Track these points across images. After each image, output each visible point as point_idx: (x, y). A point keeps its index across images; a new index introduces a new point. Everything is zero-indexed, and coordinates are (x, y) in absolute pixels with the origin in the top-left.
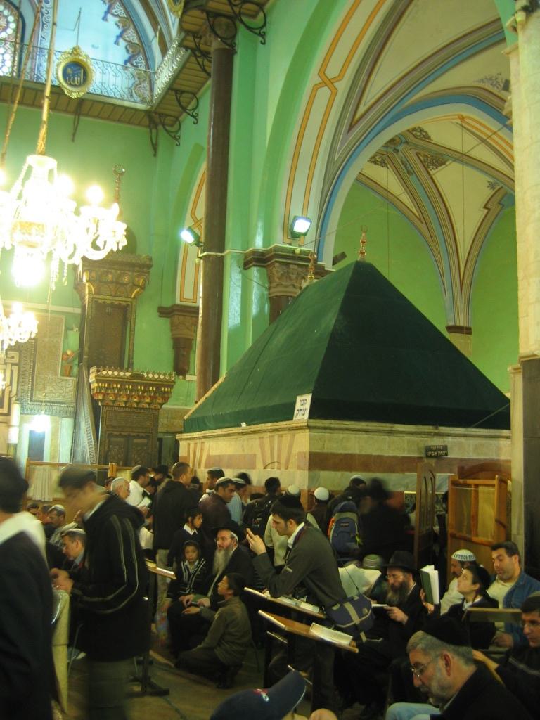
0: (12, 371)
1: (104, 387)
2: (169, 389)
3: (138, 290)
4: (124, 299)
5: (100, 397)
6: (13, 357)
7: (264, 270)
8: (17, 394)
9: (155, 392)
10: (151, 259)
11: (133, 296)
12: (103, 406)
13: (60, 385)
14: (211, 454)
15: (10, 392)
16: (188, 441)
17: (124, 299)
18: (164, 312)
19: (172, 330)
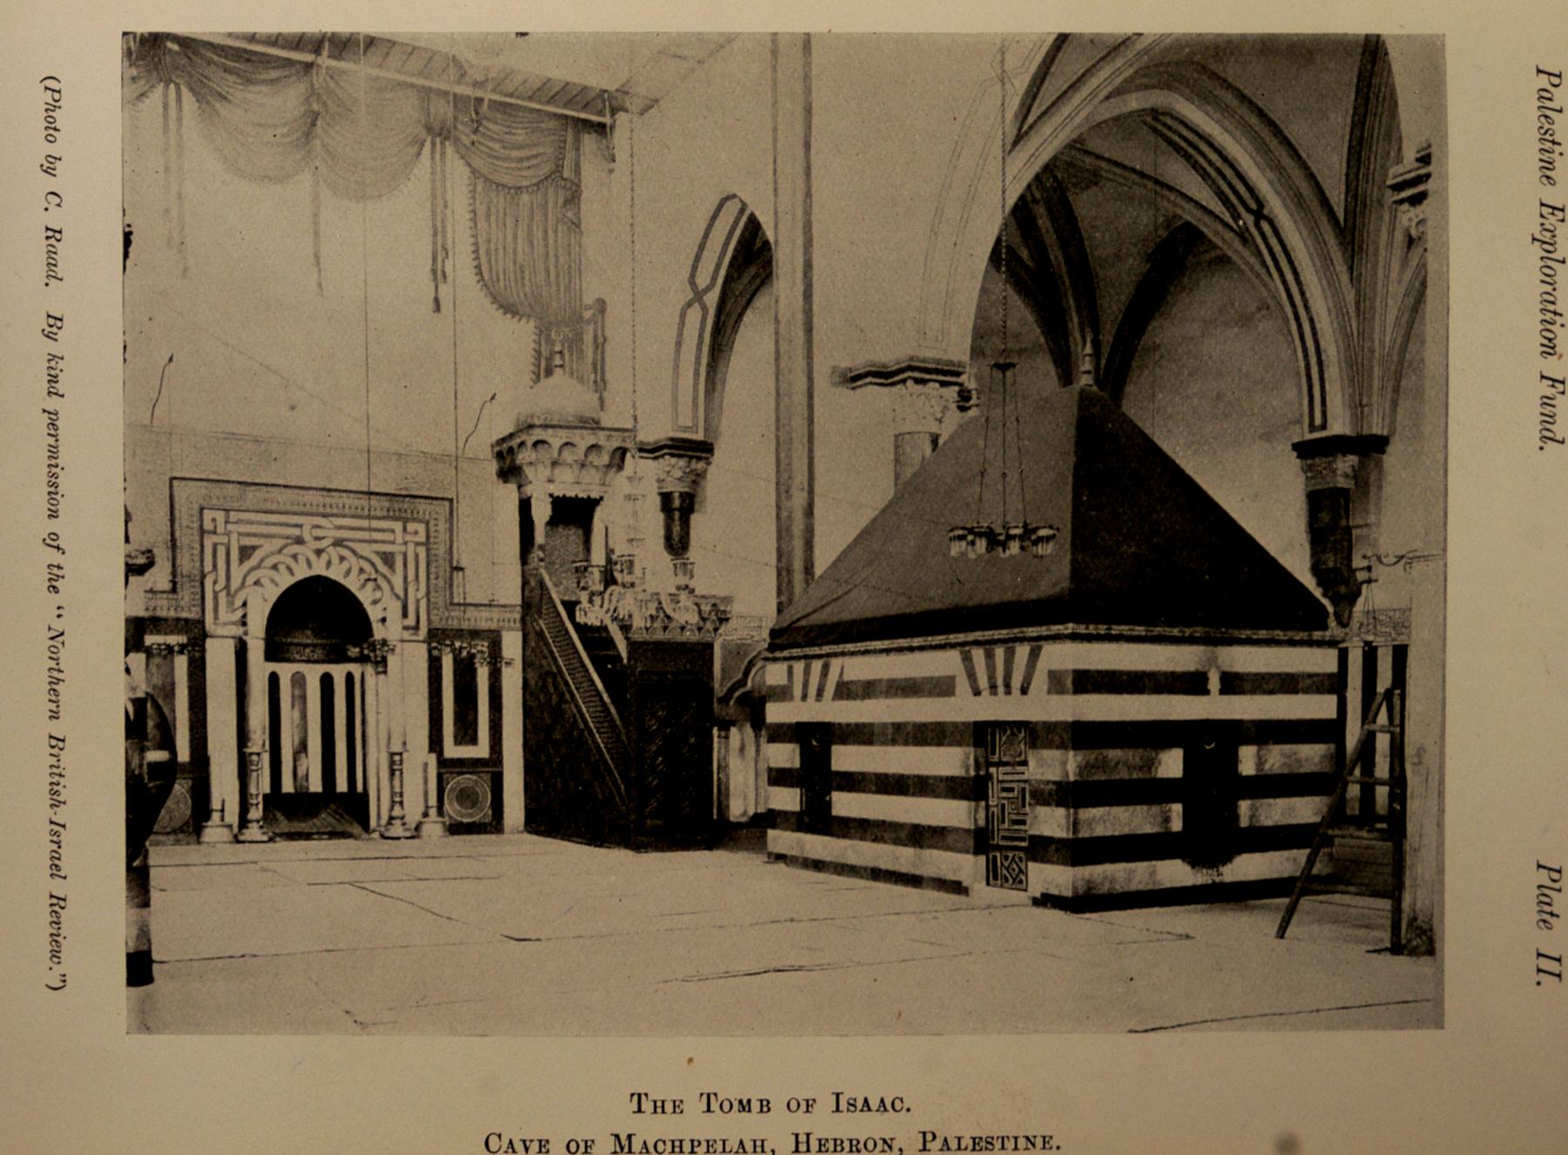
0: (417, 556)
6: (416, 533)
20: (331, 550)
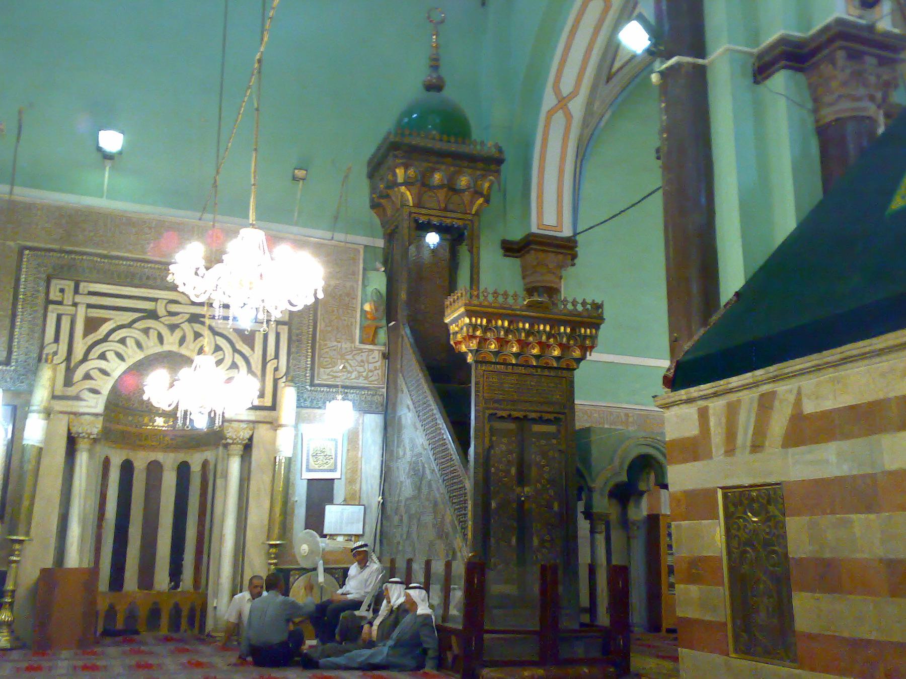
0: (278, 335)
1: (481, 325)
2: (594, 331)
3: (481, 200)
4: (459, 216)
5: (474, 345)
7: (800, 77)
8: (286, 374)
9: (569, 337)
10: (500, 150)
11: (473, 212)
12: (476, 362)
13: (359, 358)
14: (809, 407)
15: (276, 369)
16: (701, 403)
17: (459, 216)
18: (510, 249)
19: (524, 278)
20: (186, 326)
